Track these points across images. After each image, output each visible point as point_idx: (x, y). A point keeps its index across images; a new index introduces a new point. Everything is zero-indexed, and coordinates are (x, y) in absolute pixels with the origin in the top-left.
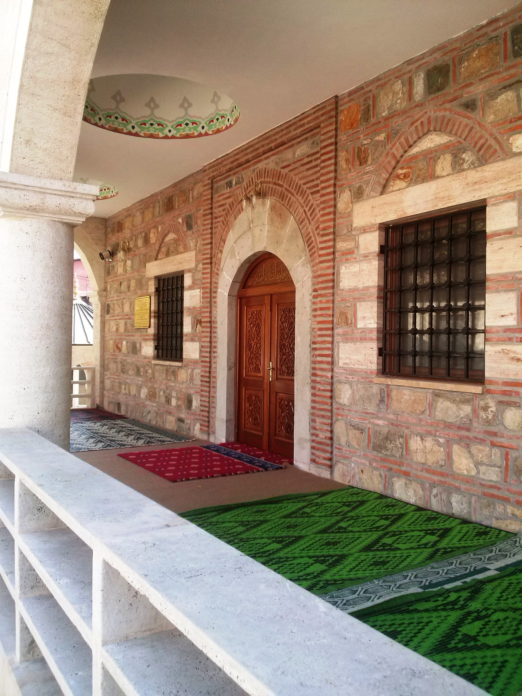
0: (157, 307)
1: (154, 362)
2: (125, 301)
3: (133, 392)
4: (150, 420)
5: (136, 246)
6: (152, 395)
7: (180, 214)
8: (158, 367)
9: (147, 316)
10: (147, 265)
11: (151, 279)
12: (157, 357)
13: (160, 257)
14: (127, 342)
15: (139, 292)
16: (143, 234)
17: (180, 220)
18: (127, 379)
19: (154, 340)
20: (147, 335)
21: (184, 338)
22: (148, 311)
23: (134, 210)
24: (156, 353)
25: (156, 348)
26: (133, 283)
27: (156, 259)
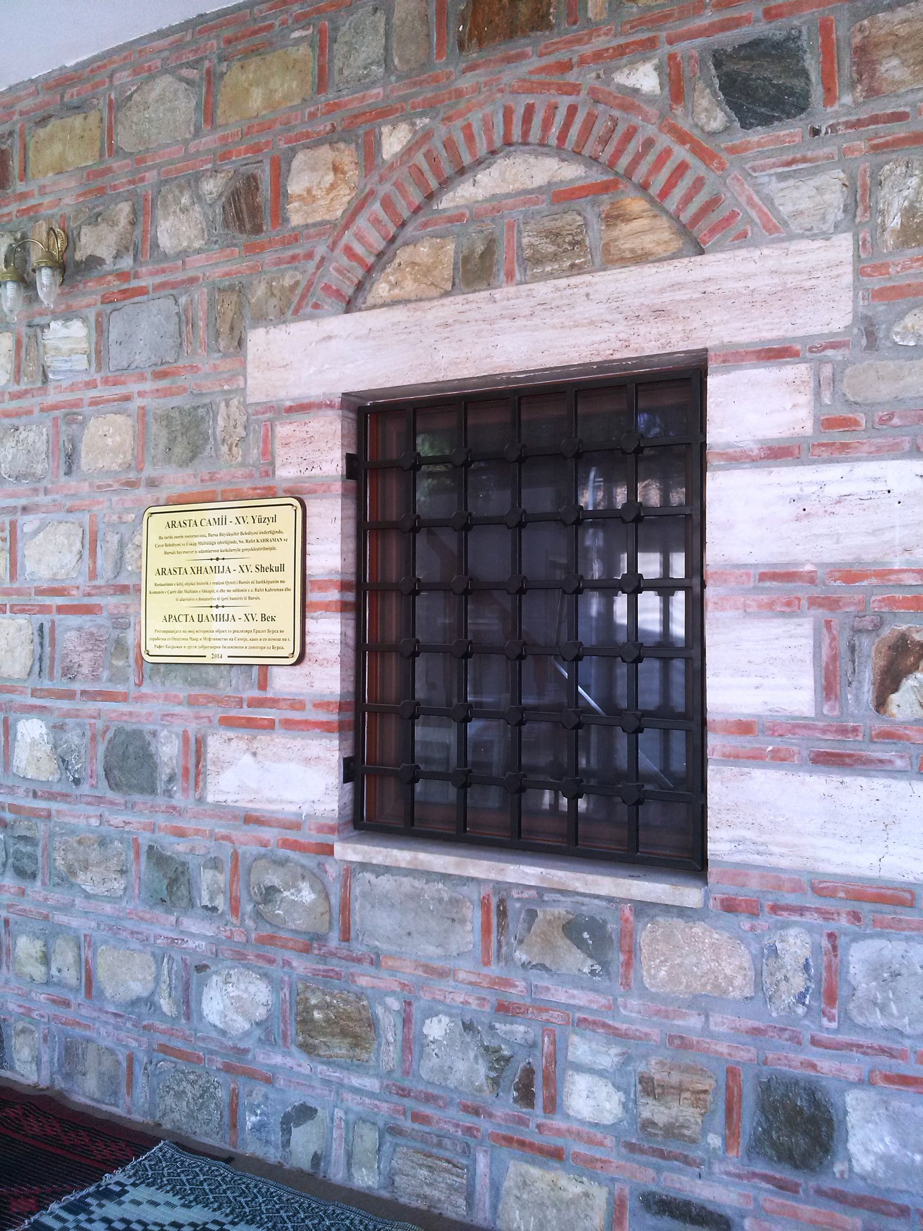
0: (351, 558)
1: (350, 851)
2: (28, 523)
3: (128, 976)
4: (316, 1159)
5: (139, 245)
6: (329, 1025)
7: (651, 43)
8: (385, 883)
9: (284, 605)
10: (259, 340)
11: (303, 408)
12: (363, 820)
13: (381, 289)
14: (58, 728)
15: (178, 479)
16: (211, 187)
17: (645, 78)
18: (66, 908)
19: (341, 727)
20: (256, 703)
21: (713, 741)
22: (289, 578)
23: (123, 77)
24: (348, 798)
25: (352, 770)
26: (108, 439)
27: (350, 306)
